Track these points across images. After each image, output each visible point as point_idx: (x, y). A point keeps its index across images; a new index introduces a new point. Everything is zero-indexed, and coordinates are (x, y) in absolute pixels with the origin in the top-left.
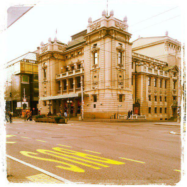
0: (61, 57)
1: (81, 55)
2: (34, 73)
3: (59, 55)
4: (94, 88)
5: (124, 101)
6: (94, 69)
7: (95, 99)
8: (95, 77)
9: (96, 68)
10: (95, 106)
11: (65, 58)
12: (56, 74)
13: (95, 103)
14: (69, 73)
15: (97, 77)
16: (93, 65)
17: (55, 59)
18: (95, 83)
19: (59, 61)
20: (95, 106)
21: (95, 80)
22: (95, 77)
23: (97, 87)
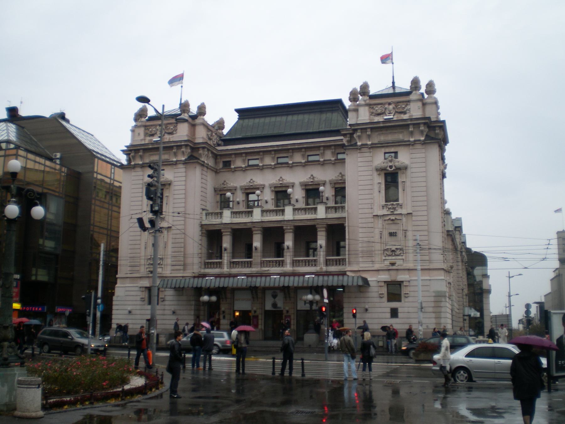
0: (210, 162)
1: (291, 167)
2: (45, 191)
3: (210, 155)
4: (393, 264)
5: (407, 300)
6: (385, 212)
7: (395, 291)
8: (392, 234)
9: (395, 213)
10: (394, 313)
11: (221, 165)
12: (203, 210)
13: (394, 305)
14: (231, 212)
15: (400, 234)
16: (384, 203)
17: (203, 165)
18: (393, 251)
19: (209, 171)
20: (394, 313)
21: (392, 244)
22: (392, 234)
23: (400, 262)
